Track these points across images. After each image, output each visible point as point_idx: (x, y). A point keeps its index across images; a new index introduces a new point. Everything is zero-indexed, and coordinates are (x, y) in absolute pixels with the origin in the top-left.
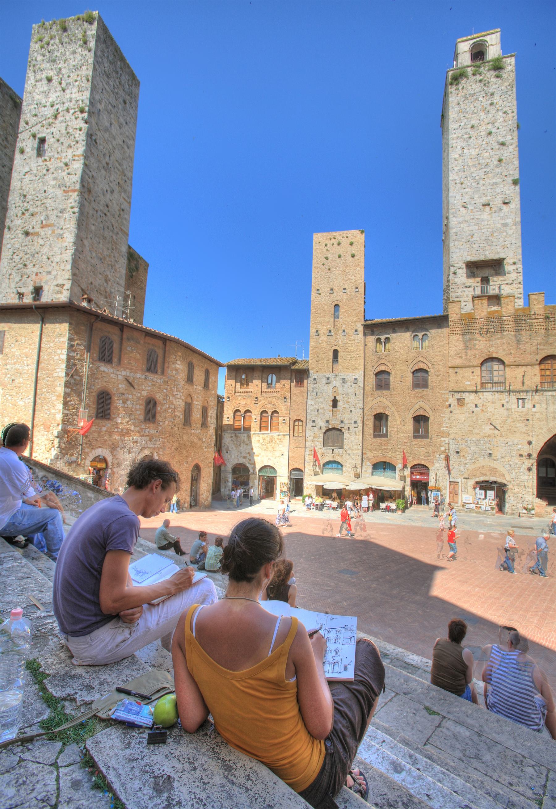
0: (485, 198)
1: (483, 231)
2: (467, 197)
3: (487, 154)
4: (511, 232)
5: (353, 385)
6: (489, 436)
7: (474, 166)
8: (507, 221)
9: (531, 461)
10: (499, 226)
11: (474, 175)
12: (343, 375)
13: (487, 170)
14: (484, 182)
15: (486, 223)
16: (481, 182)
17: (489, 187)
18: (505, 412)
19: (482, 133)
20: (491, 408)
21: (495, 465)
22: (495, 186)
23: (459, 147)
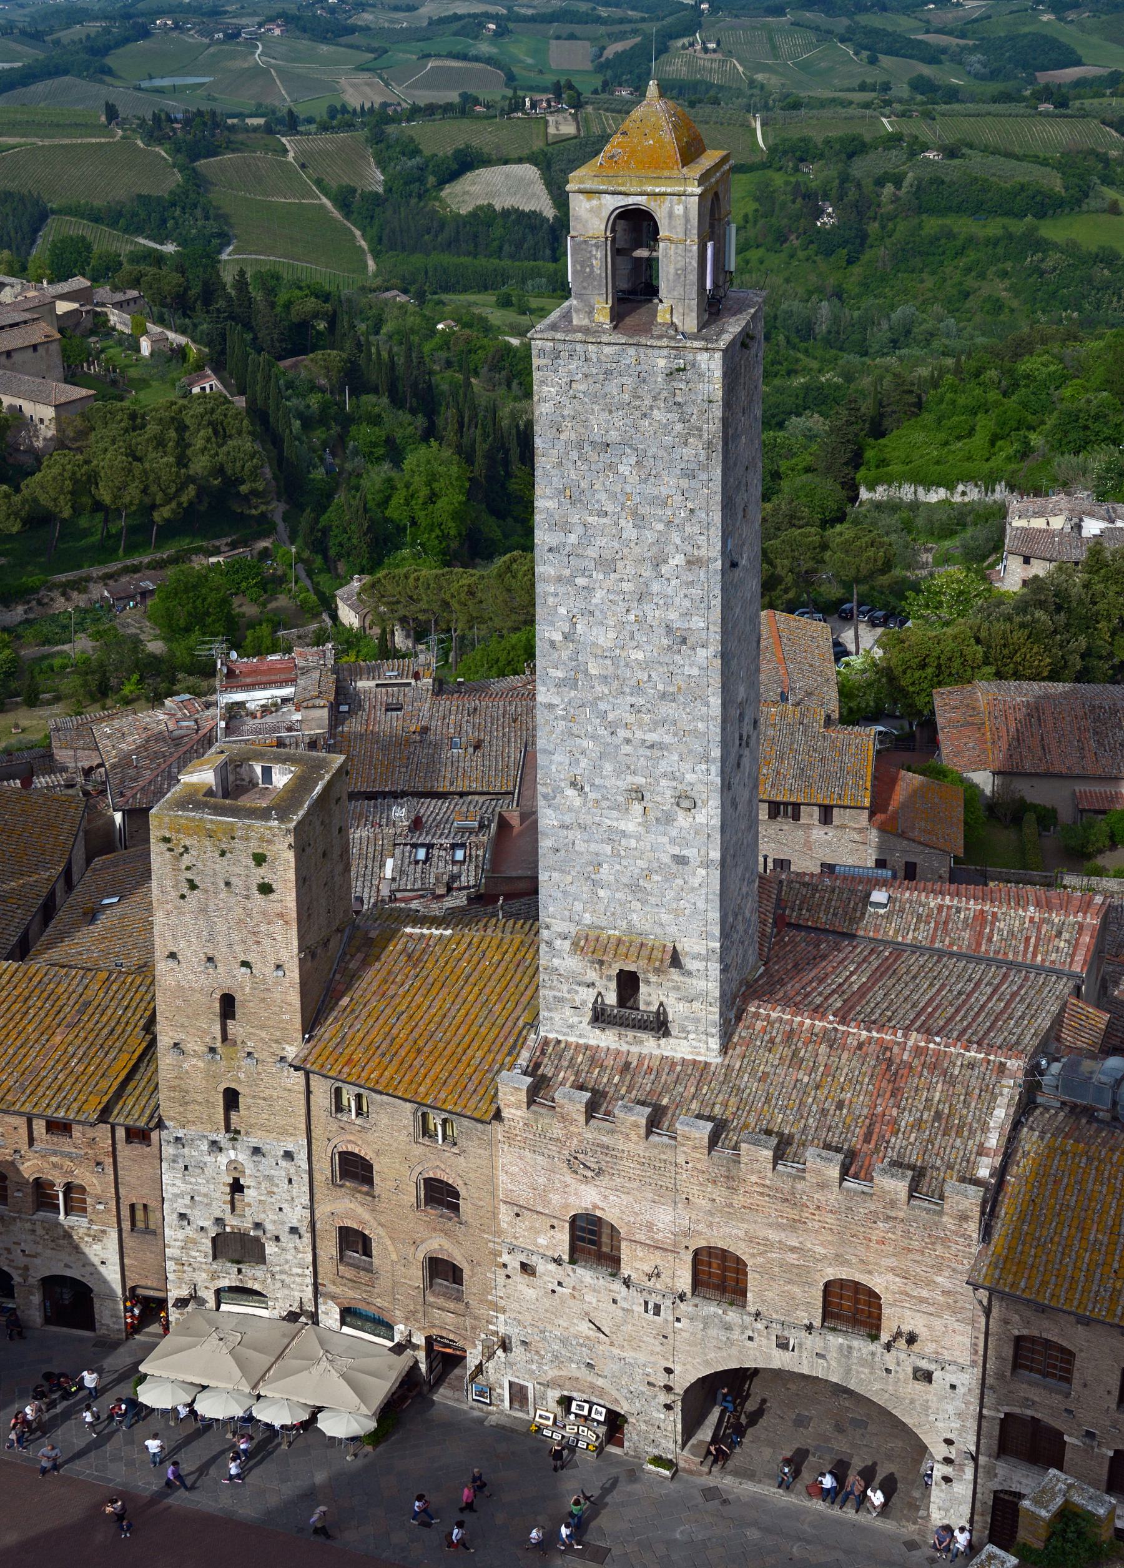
0: (630, 779)
1: (624, 862)
2: (584, 763)
3: (640, 655)
4: (696, 882)
5: (283, 1163)
6: (587, 1338)
7: (604, 679)
8: (684, 852)
9: (672, 1397)
10: (666, 859)
11: (603, 706)
12: (254, 1141)
13: (640, 701)
14: (629, 735)
15: (633, 843)
16: (622, 733)
17: (641, 751)
18: (620, 1313)
19: (626, 586)
20: (590, 1298)
21: (600, 1382)
22: (658, 753)
23: (562, 611)
